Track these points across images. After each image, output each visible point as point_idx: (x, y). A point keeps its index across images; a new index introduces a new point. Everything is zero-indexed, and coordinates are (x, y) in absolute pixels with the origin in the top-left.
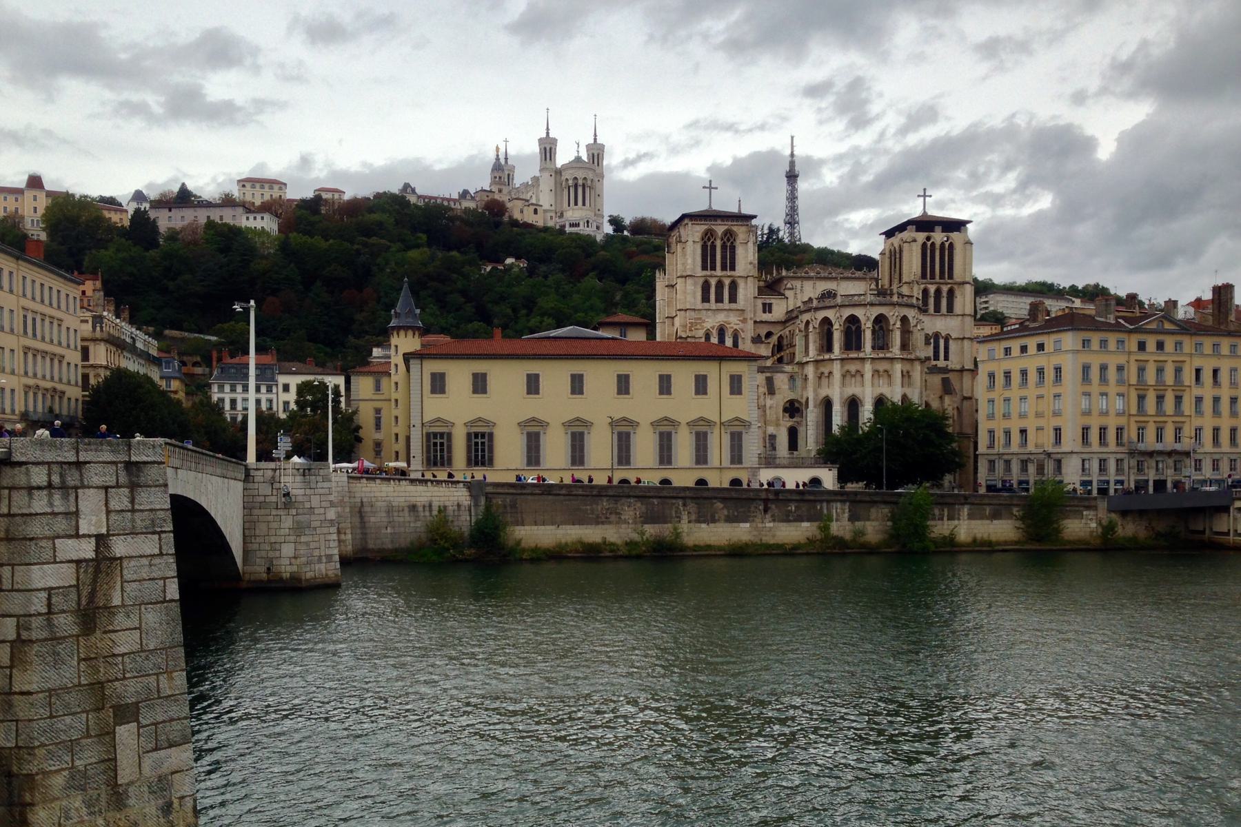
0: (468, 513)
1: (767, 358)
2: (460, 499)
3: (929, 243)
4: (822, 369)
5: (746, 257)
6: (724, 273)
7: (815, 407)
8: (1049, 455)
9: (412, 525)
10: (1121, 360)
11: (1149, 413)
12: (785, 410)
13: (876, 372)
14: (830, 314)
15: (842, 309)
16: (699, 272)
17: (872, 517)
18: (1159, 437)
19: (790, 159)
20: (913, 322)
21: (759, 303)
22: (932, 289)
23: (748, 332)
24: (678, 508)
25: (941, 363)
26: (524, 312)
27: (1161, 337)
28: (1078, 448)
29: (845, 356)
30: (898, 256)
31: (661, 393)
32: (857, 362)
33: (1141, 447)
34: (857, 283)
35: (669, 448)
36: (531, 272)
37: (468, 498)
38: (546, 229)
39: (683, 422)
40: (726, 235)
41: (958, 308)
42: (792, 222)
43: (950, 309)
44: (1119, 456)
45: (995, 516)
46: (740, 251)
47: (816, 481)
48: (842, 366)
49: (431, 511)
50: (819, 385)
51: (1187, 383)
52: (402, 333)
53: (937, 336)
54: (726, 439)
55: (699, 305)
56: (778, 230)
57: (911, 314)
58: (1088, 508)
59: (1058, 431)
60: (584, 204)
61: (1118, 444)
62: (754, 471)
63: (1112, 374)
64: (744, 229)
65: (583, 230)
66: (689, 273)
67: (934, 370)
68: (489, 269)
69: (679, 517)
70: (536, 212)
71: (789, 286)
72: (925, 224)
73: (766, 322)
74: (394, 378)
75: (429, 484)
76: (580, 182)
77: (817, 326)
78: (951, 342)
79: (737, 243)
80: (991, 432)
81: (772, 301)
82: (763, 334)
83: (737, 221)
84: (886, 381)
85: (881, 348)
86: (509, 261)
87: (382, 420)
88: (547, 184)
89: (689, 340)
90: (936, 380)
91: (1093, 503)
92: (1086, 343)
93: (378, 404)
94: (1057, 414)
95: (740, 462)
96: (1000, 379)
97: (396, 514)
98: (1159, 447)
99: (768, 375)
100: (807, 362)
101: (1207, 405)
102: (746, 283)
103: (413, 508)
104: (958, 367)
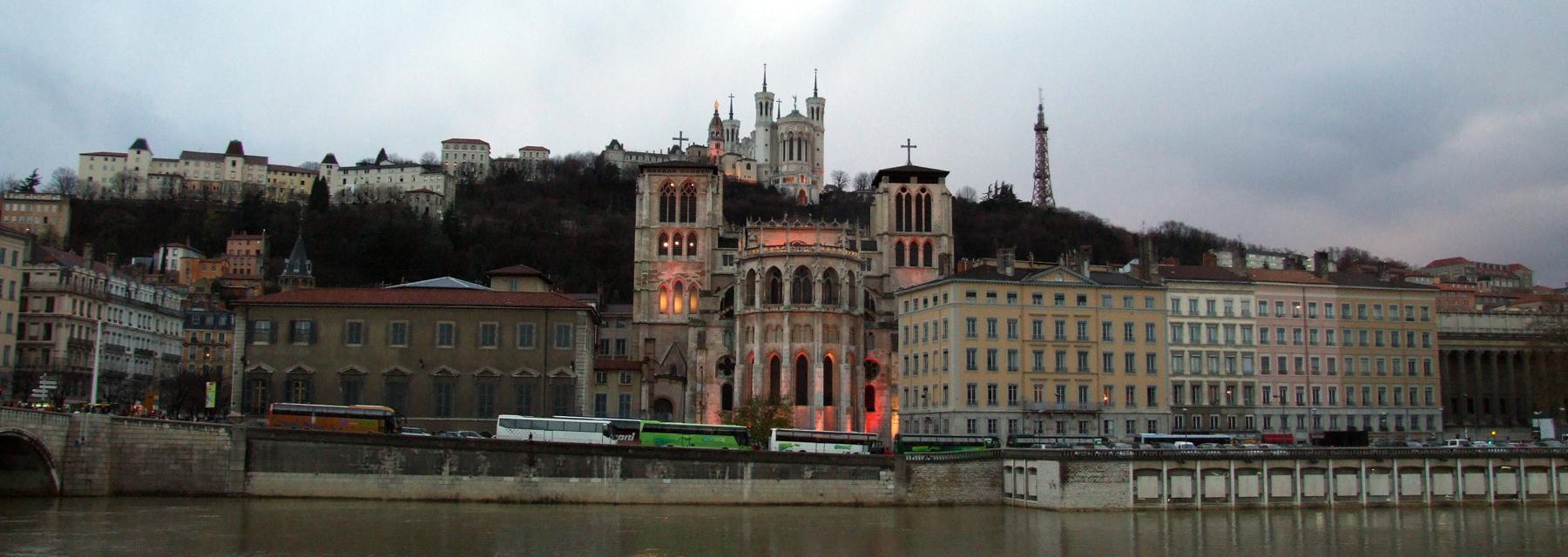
1: (716, 312)
3: (904, 194)
5: (709, 206)
10: (1014, 313)
12: (720, 366)
15: (764, 260)
19: (1038, 112)
21: (719, 254)
22: (907, 242)
27: (1059, 291)
28: (964, 408)
32: (778, 315)
33: (1039, 407)
40: (686, 186)
42: (1042, 175)
44: (1012, 417)
46: (699, 203)
48: (763, 320)
50: (747, 341)
51: (1094, 339)
60: (799, 158)
64: (703, 179)
66: (644, 224)
69: (441, 469)
70: (749, 167)
75: (191, 427)
76: (795, 136)
77: (745, 278)
88: (763, 138)
99: (701, 329)
101: (1119, 363)
102: (705, 234)
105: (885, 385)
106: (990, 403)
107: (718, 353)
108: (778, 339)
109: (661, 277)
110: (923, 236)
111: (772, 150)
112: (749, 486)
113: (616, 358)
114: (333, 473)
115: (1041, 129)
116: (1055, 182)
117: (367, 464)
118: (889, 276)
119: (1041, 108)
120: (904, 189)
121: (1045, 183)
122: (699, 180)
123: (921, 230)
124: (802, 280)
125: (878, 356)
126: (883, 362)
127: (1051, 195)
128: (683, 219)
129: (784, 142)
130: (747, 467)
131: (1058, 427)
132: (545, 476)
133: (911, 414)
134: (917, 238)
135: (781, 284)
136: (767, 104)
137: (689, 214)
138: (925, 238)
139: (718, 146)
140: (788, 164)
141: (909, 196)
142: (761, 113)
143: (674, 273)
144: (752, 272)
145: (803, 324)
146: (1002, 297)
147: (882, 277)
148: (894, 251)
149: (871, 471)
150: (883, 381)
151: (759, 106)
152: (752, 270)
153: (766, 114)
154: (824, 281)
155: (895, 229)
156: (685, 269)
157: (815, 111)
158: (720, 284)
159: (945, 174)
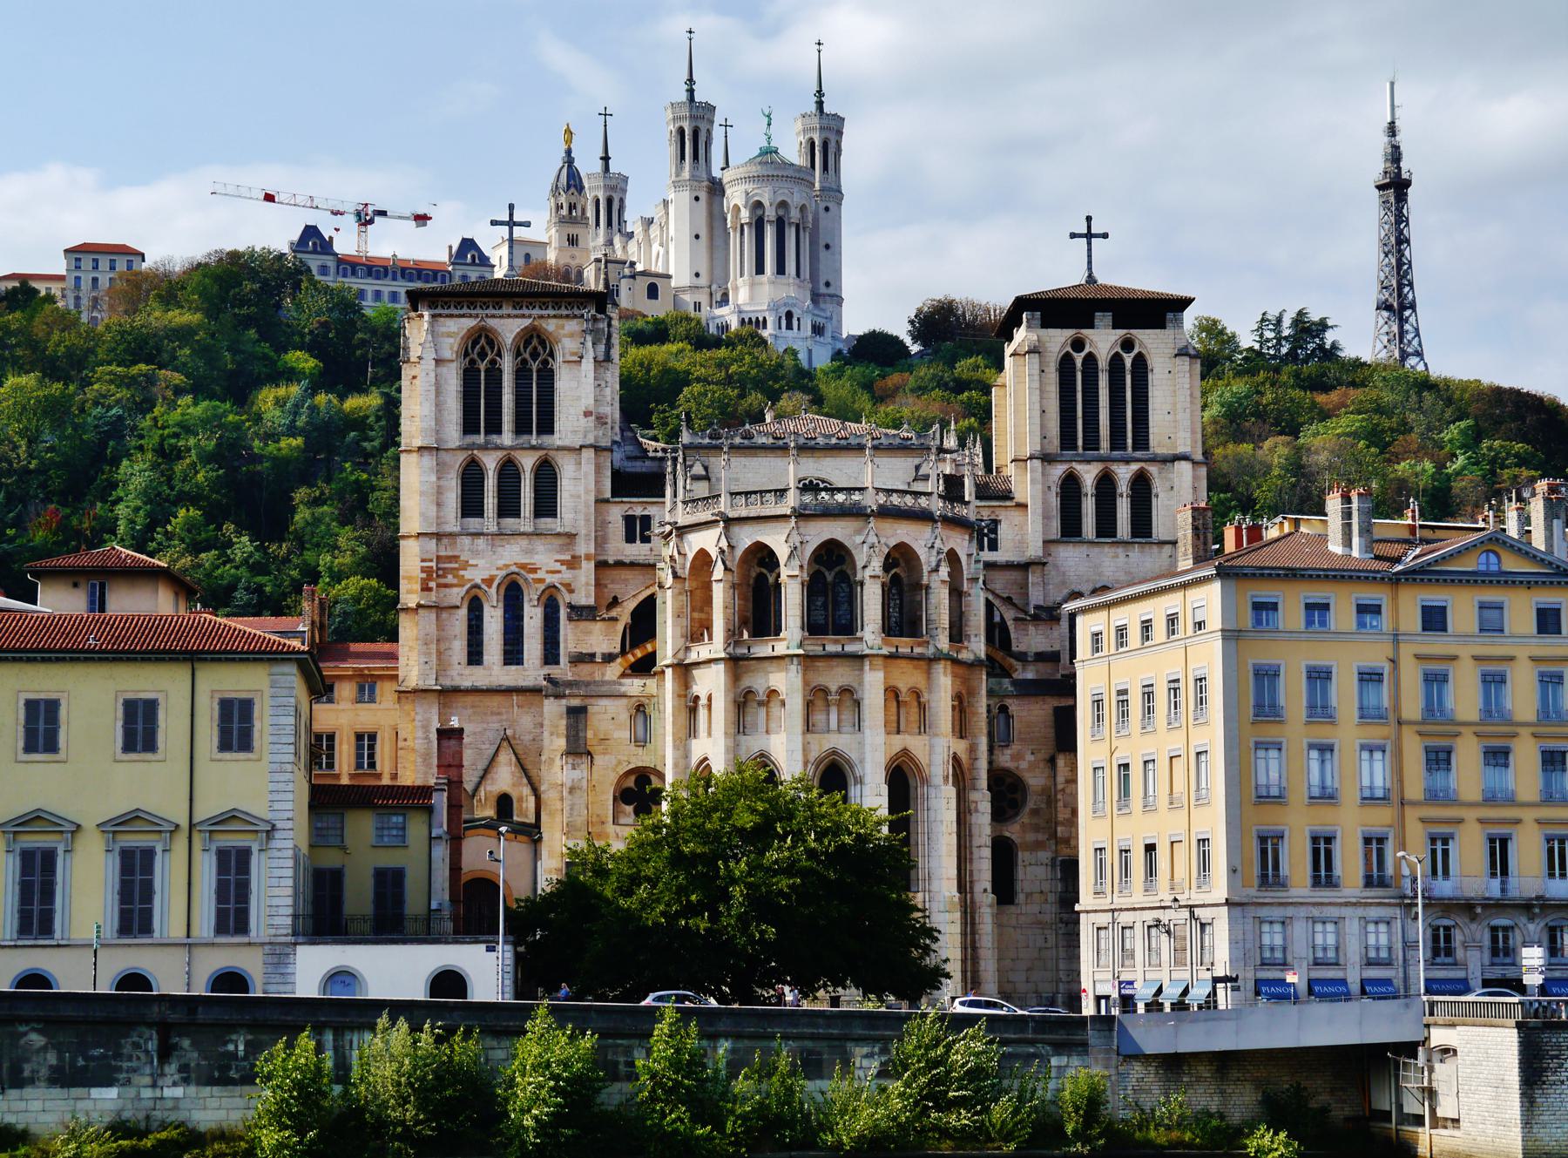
1: (609, 658)
3: (1079, 358)
10: (1375, 655)
13: (816, 698)
14: (708, 540)
15: (736, 530)
16: (453, 433)
21: (616, 514)
22: (1089, 475)
27: (1491, 595)
31: (30, 747)
40: (527, 343)
41: (1160, 529)
43: (1142, 525)
47: (449, 982)
50: (692, 731)
56: (1323, 326)
58: (1061, 1048)
61: (1369, 882)
62: (279, 956)
63: (1344, 693)
64: (573, 326)
70: (653, 292)
73: (633, 565)
76: (770, 213)
77: (685, 572)
81: (651, 511)
83: (557, 306)
84: (847, 716)
95: (242, 927)
105: (1041, 837)
106: (1316, 881)
107: (619, 763)
108: (773, 725)
109: (467, 574)
110: (1127, 461)
113: (352, 776)
115: (1396, 186)
116: (1426, 317)
118: (1044, 564)
119: (1392, 130)
120: (1078, 344)
121: (1402, 321)
122: (563, 327)
124: (830, 577)
125: (1023, 765)
126: (1035, 780)
127: (1419, 354)
129: (742, 225)
131: (1494, 939)
133: (1113, 911)
135: (778, 586)
138: (1135, 467)
139: (573, 241)
141: (1091, 360)
142: (683, 157)
143: (501, 563)
144: (703, 558)
145: (833, 688)
146: (1343, 615)
147: (1024, 567)
148: (1055, 502)
149: (1034, 1056)
150: (1036, 828)
151: (675, 138)
152: (703, 555)
154: (887, 579)
155: (1056, 442)
156: (528, 552)
158: (614, 589)
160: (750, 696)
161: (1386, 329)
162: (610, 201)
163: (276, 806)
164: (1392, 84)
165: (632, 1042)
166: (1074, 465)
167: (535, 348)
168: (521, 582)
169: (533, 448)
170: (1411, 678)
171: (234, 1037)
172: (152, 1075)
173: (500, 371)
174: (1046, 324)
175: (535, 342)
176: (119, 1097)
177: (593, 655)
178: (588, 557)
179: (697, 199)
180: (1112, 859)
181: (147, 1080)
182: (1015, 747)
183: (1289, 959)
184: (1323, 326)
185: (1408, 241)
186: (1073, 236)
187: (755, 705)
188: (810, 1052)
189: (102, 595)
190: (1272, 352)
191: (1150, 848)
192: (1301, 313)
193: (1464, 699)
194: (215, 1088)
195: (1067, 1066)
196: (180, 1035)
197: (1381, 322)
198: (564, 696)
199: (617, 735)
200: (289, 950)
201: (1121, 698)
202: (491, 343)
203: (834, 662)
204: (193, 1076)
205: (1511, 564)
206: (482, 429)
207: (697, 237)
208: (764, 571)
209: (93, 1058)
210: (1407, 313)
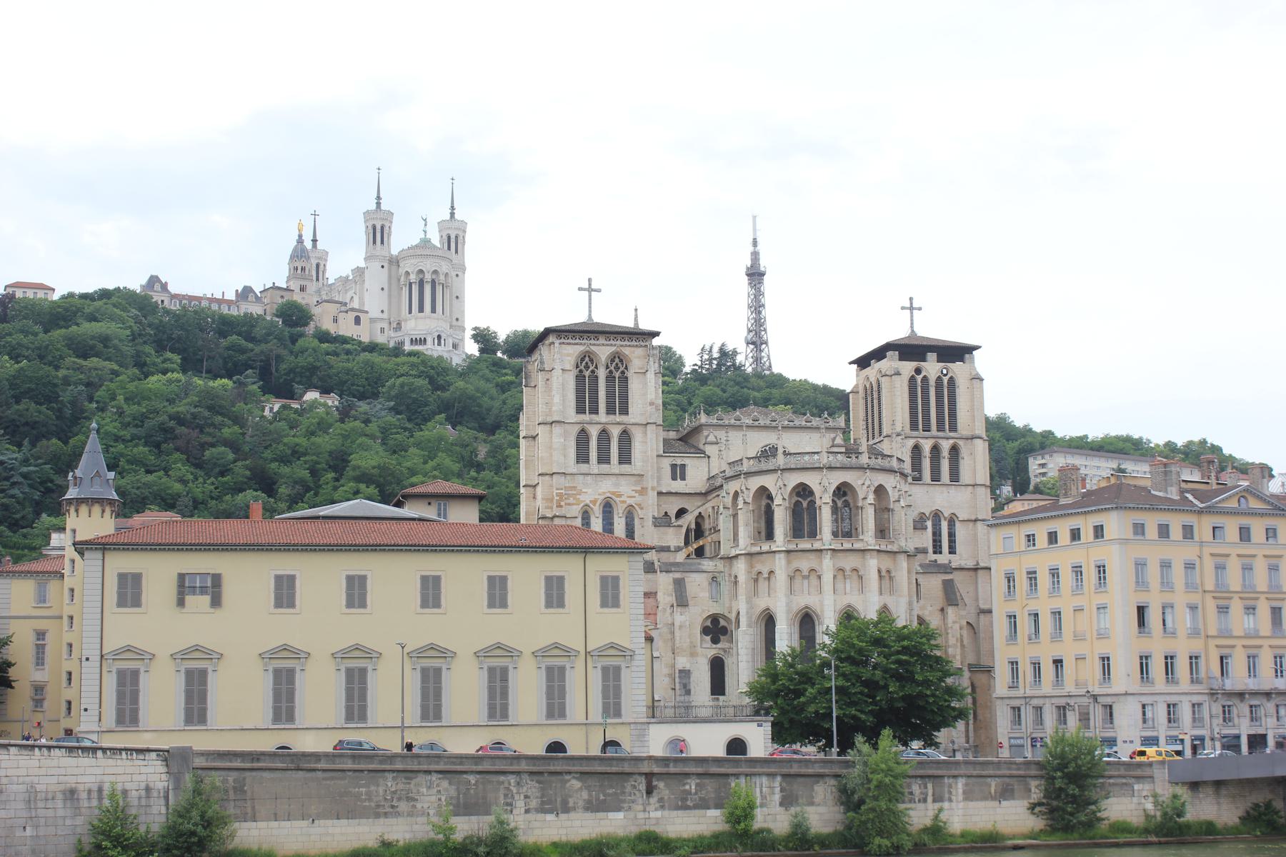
0: (162, 802)
1: (678, 549)
2: (152, 778)
3: (919, 378)
4: (758, 567)
6: (611, 418)
7: (749, 626)
8: (1095, 697)
9: (68, 822)
11: (1235, 634)
12: (705, 631)
14: (769, 482)
15: (787, 475)
16: (572, 415)
17: (817, 800)
18: (1252, 670)
19: (752, 249)
20: (893, 495)
21: (666, 463)
22: (927, 446)
23: (650, 508)
24: (508, 789)
25: (943, 558)
26: (331, 475)
27: (1245, 521)
29: (792, 547)
30: (875, 396)
31: (491, 604)
32: (812, 556)
33: (1229, 685)
34: (815, 436)
35: (505, 694)
36: (345, 413)
37: (164, 777)
38: (372, 348)
39: (527, 652)
40: (613, 361)
41: (965, 476)
43: (955, 476)
44: (1196, 699)
45: (1005, 793)
46: (634, 385)
47: (736, 746)
48: (789, 562)
49: (100, 798)
50: (756, 593)
52: (84, 509)
53: (937, 516)
54: (596, 678)
55: (572, 466)
56: (735, 353)
57: (889, 482)
58: (1139, 778)
59: (1105, 660)
60: (433, 310)
61: (1192, 682)
62: (640, 729)
63: (1178, 572)
64: (640, 351)
65: (431, 349)
66: (556, 418)
67: (935, 568)
68: (276, 408)
69: (511, 805)
70: (357, 321)
71: (711, 438)
72: (911, 350)
73: (676, 494)
74: (68, 582)
75: (100, 753)
76: (428, 277)
77: (750, 500)
78: (958, 525)
79: (630, 374)
80: (1014, 664)
81: (686, 461)
82: (672, 514)
85: (848, 535)
86: (311, 396)
87: (47, 648)
88: (377, 278)
89: (557, 521)
90: (933, 584)
91: (1147, 772)
92: (1139, 529)
93: (41, 625)
94: (1102, 636)
96: (1022, 583)
97: (41, 804)
98: (1252, 684)
99: (678, 575)
100: (736, 556)
103: (71, 794)
104: (970, 564)
107: (703, 611)
109: (582, 497)
110: (948, 438)
111: (390, 296)
112: (960, 812)
114: (338, 819)
115: (755, 275)
117: (395, 803)
119: (755, 243)
123: (944, 431)
124: (840, 503)
125: (927, 613)
128: (610, 410)
129: (411, 284)
130: (956, 783)
131: (1251, 711)
132: (669, 809)
133: (1025, 697)
134: (940, 441)
136: (382, 228)
137: (619, 404)
138: (951, 441)
140: (416, 319)
141: (925, 379)
142: (374, 242)
143: (601, 491)
149: (1126, 784)
151: (371, 231)
153: (382, 242)
157: (453, 241)
159: (970, 349)
160: (798, 573)
161: (751, 355)
162: (318, 266)
163: (635, 640)
164: (754, 217)
165: (913, 780)
166: (919, 439)
167: (617, 364)
168: (612, 502)
169: (618, 423)
170: (1209, 564)
171: (689, 781)
172: (643, 804)
173: (597, 377)
174: (902, 358)
175: (617, 360)
176: (625, 818)
177: (669, 547)
178: (653, 489)
179: (383, 267)
180: (1026, 669)
181: (641, 807)
182: (922, 602)
183: (1156, 725)
184: (735, 353)
185: (763, 305)
186: (903, 308)
187: (801, 578)
188: (1008, 785)
189: (445, 510)
190: (707, 366)
191: (1058, 663)
192: (723, 345)
193: (1234, 579)
194: (679, 812)
195: (1143, 790)
196: (658, 780)
197: (749, 351)
198: (671, 572)
199: (702, 595)
200: (645, 726)
201: (1030, 576)
202: (592, 361)
203: (848, 554)
204: (666, 804)
205: (1254, 504)
206: (587, 412)
207: (383, 289)
208: (800, 499)
209: (609, 795)
210: (764, 346)
